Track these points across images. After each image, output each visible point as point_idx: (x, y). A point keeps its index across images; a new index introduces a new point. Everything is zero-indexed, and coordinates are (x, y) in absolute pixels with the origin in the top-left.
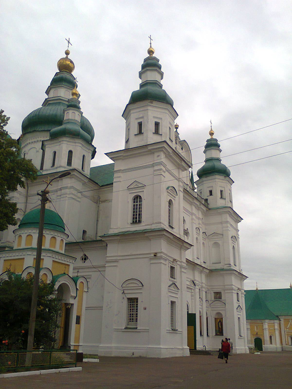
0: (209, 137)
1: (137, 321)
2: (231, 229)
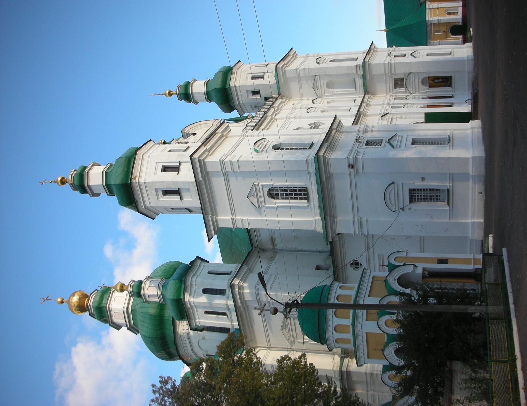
0: (175, 97)
1: (439, 190)
2: (306, 66)
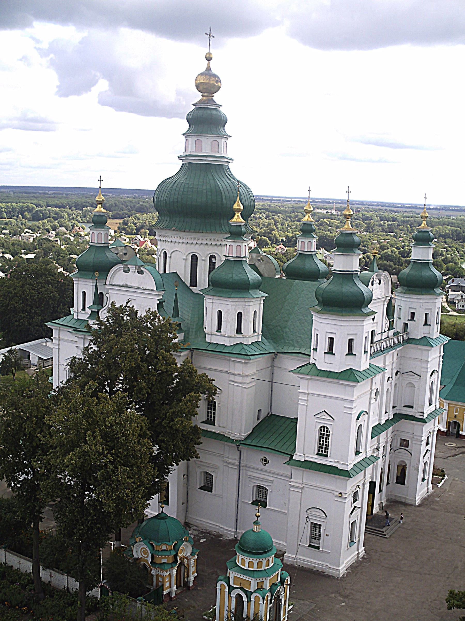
1: (319, 540)
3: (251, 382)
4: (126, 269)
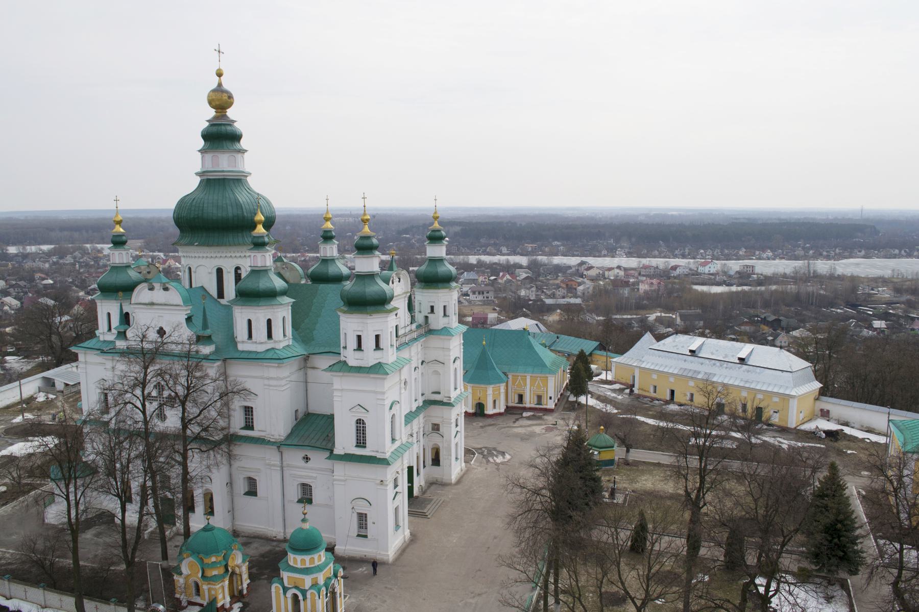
1: (366, 529)
3: (285, 385)
4: (151, 287)
